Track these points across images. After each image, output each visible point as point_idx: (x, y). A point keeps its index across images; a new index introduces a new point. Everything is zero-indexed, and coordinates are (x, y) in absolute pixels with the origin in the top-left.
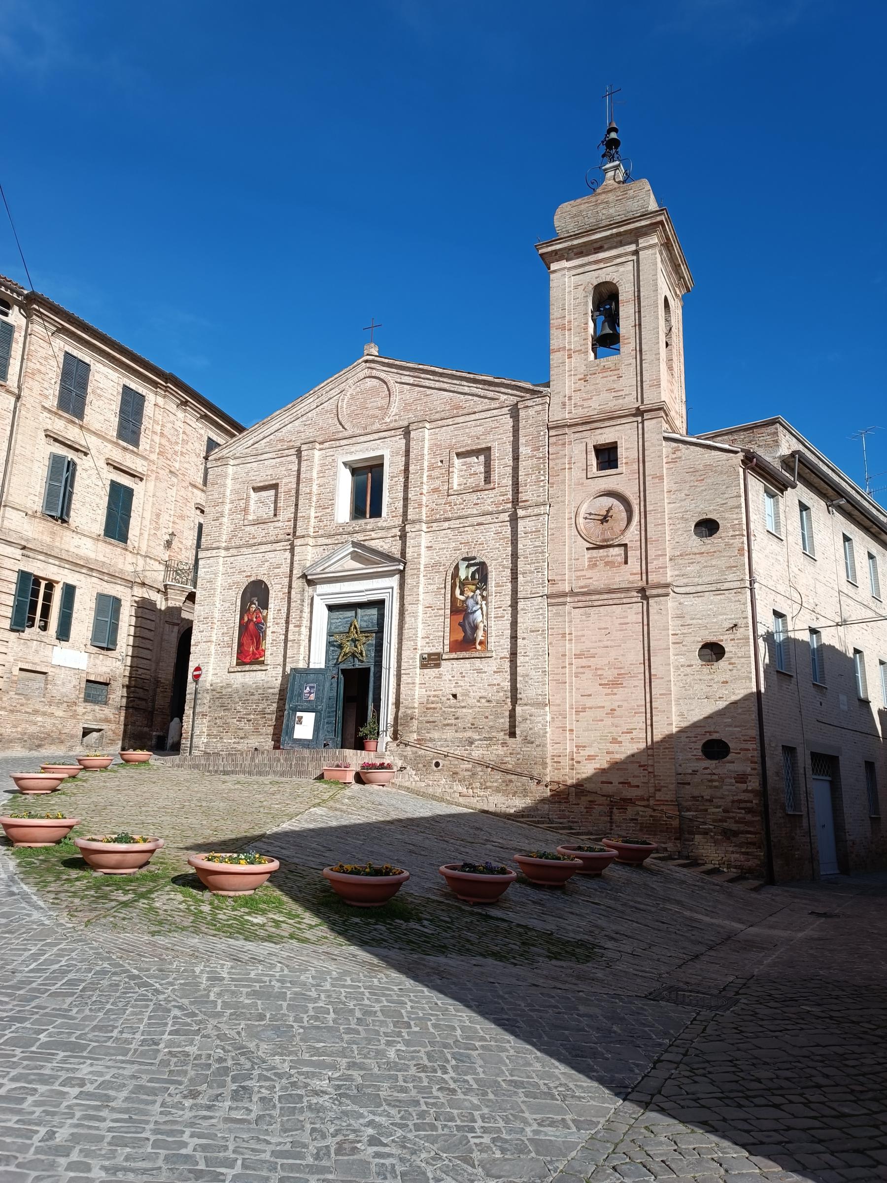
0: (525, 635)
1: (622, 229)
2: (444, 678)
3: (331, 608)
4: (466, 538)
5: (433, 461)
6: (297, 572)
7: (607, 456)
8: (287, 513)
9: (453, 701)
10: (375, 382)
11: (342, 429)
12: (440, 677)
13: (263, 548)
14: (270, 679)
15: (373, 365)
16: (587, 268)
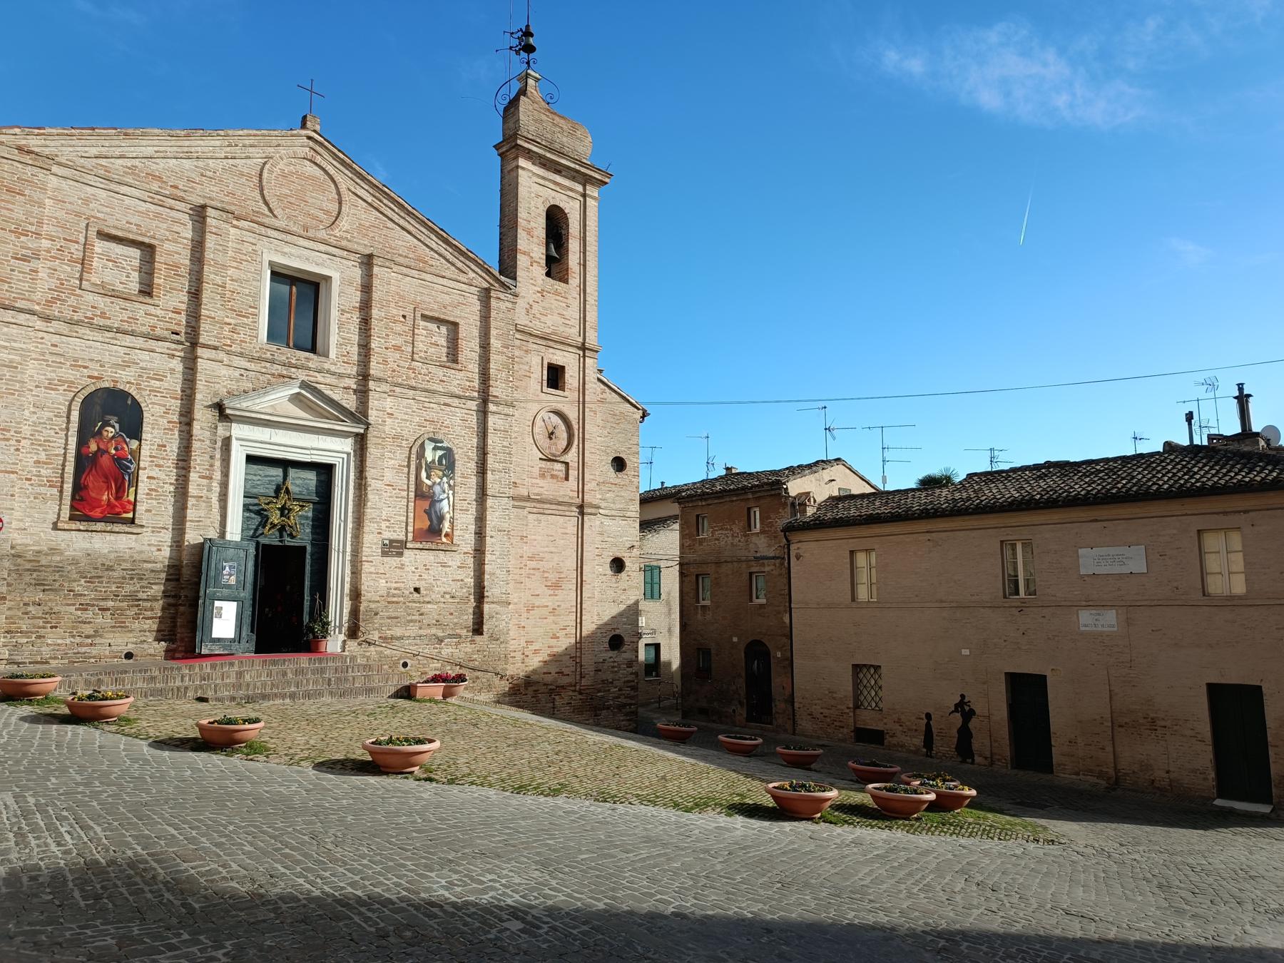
0: (493, 534)
1: (583, 170)
2: (407, 569)
3: (251, 459)
4: (431, 415)
5: (395, 312)
6: (203, 397)
7: (555, 376)
8: (172, 298)
9: (416, 595)
10: (318, 172)
12: (402, 567)
13: (128, 340)
14: (146, 548)
15: (318, 148)
16: (547, 183)
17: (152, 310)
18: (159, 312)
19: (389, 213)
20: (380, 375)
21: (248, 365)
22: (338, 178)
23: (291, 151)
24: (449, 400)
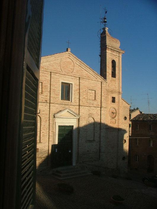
7: (113, 100)
11: (61, 71)
17: (42, 96)
18: (43, 97)
19: (83, 67)
20: (82, 105)
21: (58, 106)
22: (74, 61)
23: (65, 57)
24: (93, 108)
